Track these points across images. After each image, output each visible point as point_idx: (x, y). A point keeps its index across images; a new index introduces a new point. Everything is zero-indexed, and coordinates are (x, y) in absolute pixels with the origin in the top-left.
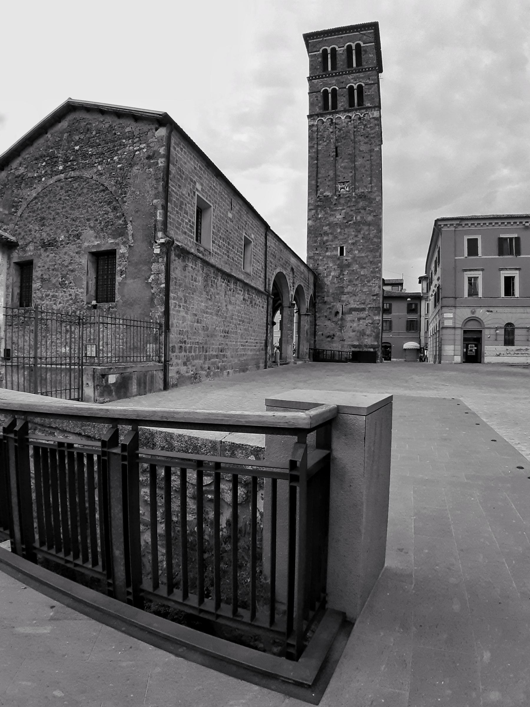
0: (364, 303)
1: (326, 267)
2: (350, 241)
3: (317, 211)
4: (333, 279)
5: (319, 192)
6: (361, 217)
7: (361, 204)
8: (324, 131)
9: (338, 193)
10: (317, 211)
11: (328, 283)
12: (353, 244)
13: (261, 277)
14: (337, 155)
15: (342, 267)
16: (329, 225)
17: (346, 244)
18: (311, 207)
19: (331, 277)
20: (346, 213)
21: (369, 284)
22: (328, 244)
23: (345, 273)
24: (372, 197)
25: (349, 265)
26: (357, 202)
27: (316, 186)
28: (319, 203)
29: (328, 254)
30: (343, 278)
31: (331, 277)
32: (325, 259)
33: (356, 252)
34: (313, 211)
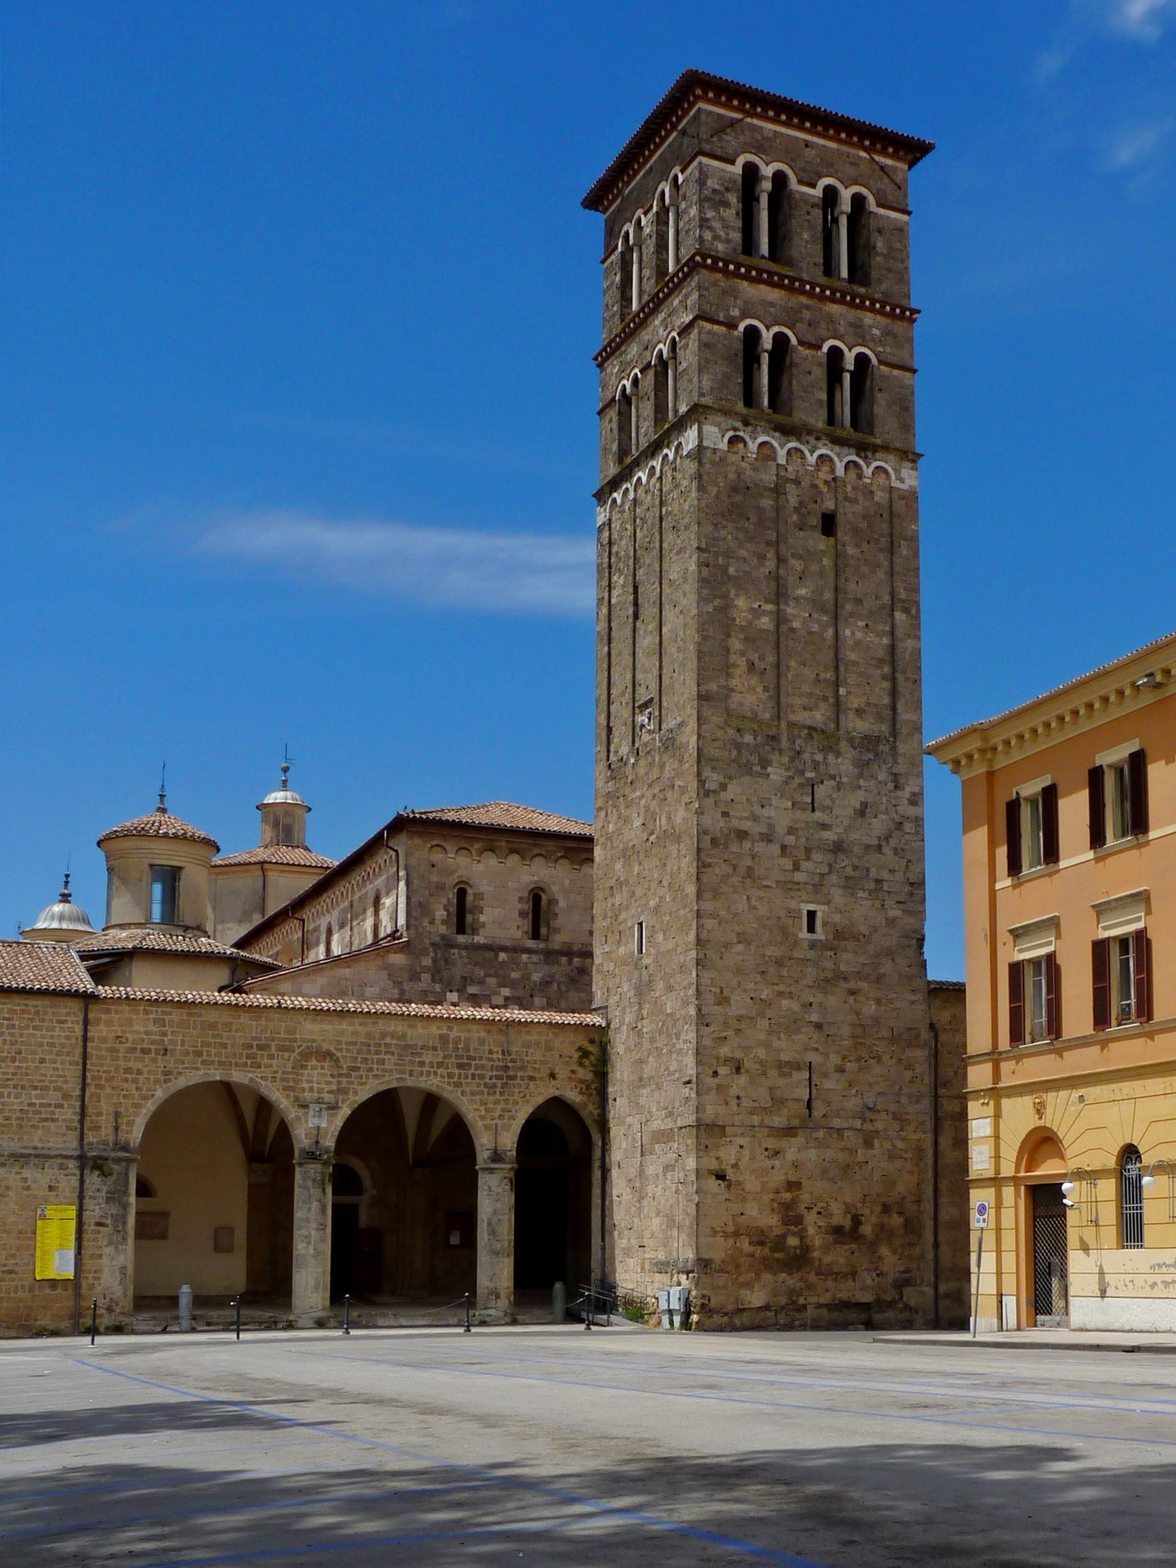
0: (671, 1114)
1: (618, 996)
2: (652, 903)
3: (607, 813)
4: (628, 1037)
5: (612, 749)
6: (669, 818)
7: (671, 765)
8: (621, 539)
9: (637, 745)
10: (607, 813)
11: (621, 1049)
12: (656, 910)
13: (53, 1120)
14: (636, 616)
15: (643, 989)
16: (624, 854)
17: (646, 913)
18: (600, 802)
19: (625, 1027)
20: (647, 809)
21: (678, 1047)
22: (621, 918)
23: (645, 1013)
24: (684, 740)
25: (650, 984)
26: (662, 766)
27: (605, 730)
28: (611, 786)
29: (622, 950)
30: (641, 1030)
31: (625, 1027)
32: (617, 970)
33: (660, 937)
34: (603, 813)
